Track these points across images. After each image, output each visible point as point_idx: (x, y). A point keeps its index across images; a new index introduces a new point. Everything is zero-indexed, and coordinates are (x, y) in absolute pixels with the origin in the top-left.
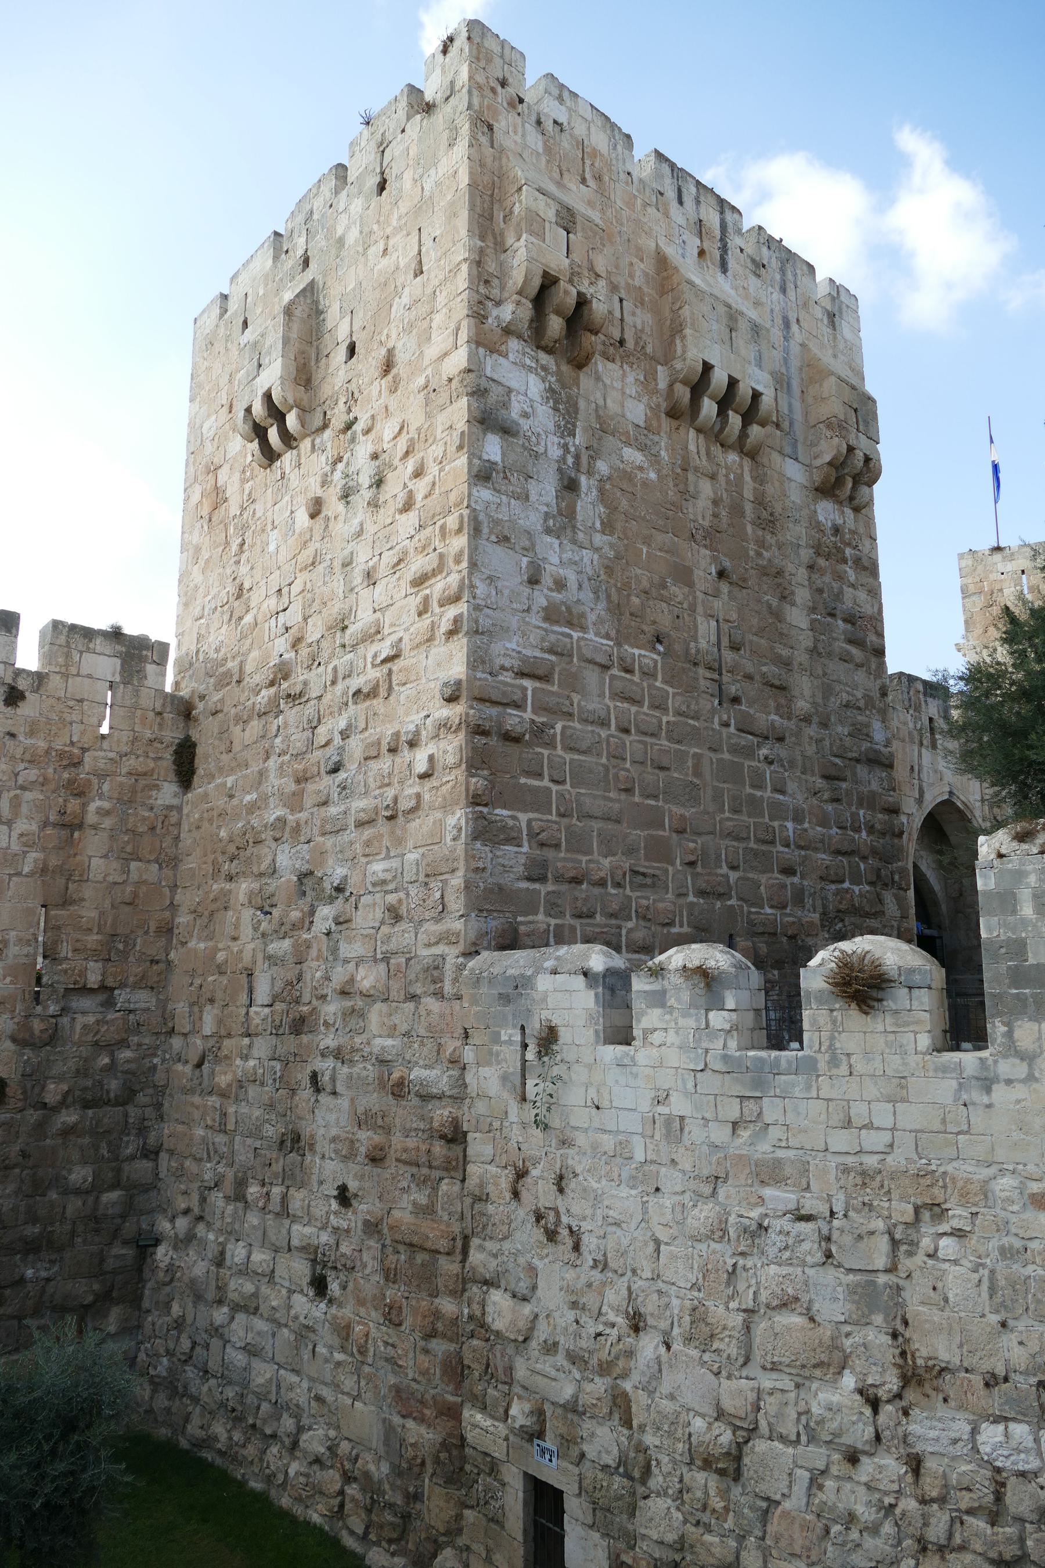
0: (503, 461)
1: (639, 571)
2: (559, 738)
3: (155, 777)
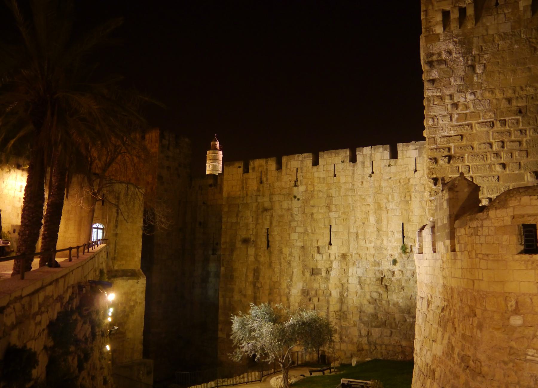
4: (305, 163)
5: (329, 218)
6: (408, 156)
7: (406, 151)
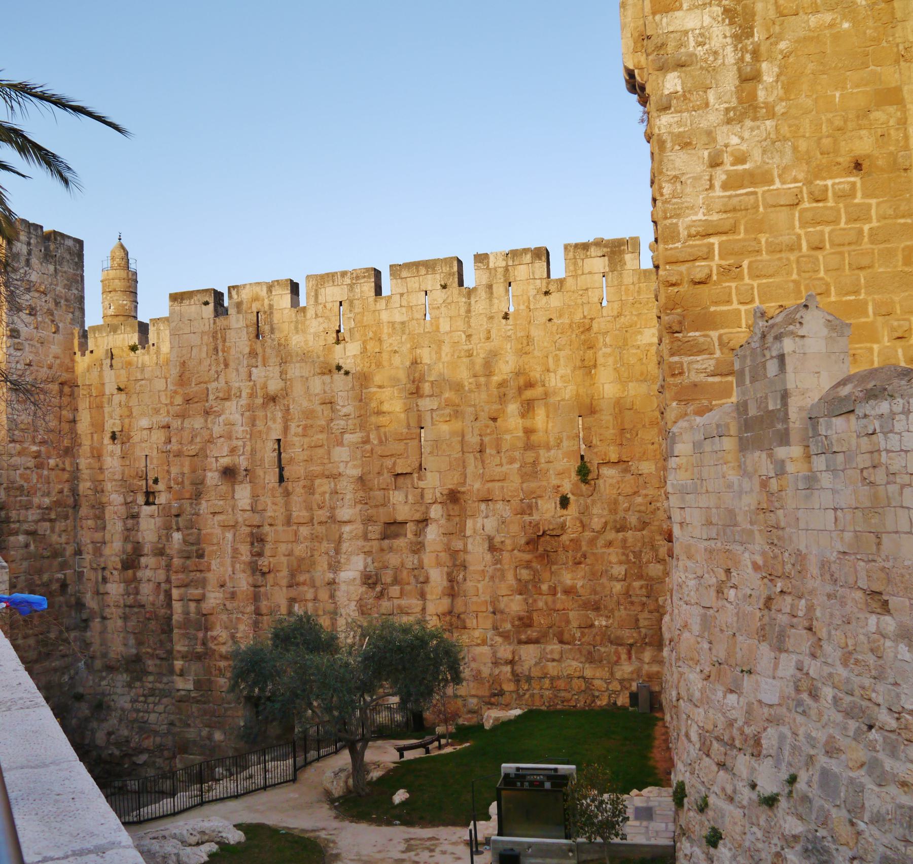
0: (683, 88)
1: (830, 115)
2: (746, 271)
3: (638, 326)
4: (358, 290)
5: (418, 411)
6: (586, 271)
7: (583, 260)
